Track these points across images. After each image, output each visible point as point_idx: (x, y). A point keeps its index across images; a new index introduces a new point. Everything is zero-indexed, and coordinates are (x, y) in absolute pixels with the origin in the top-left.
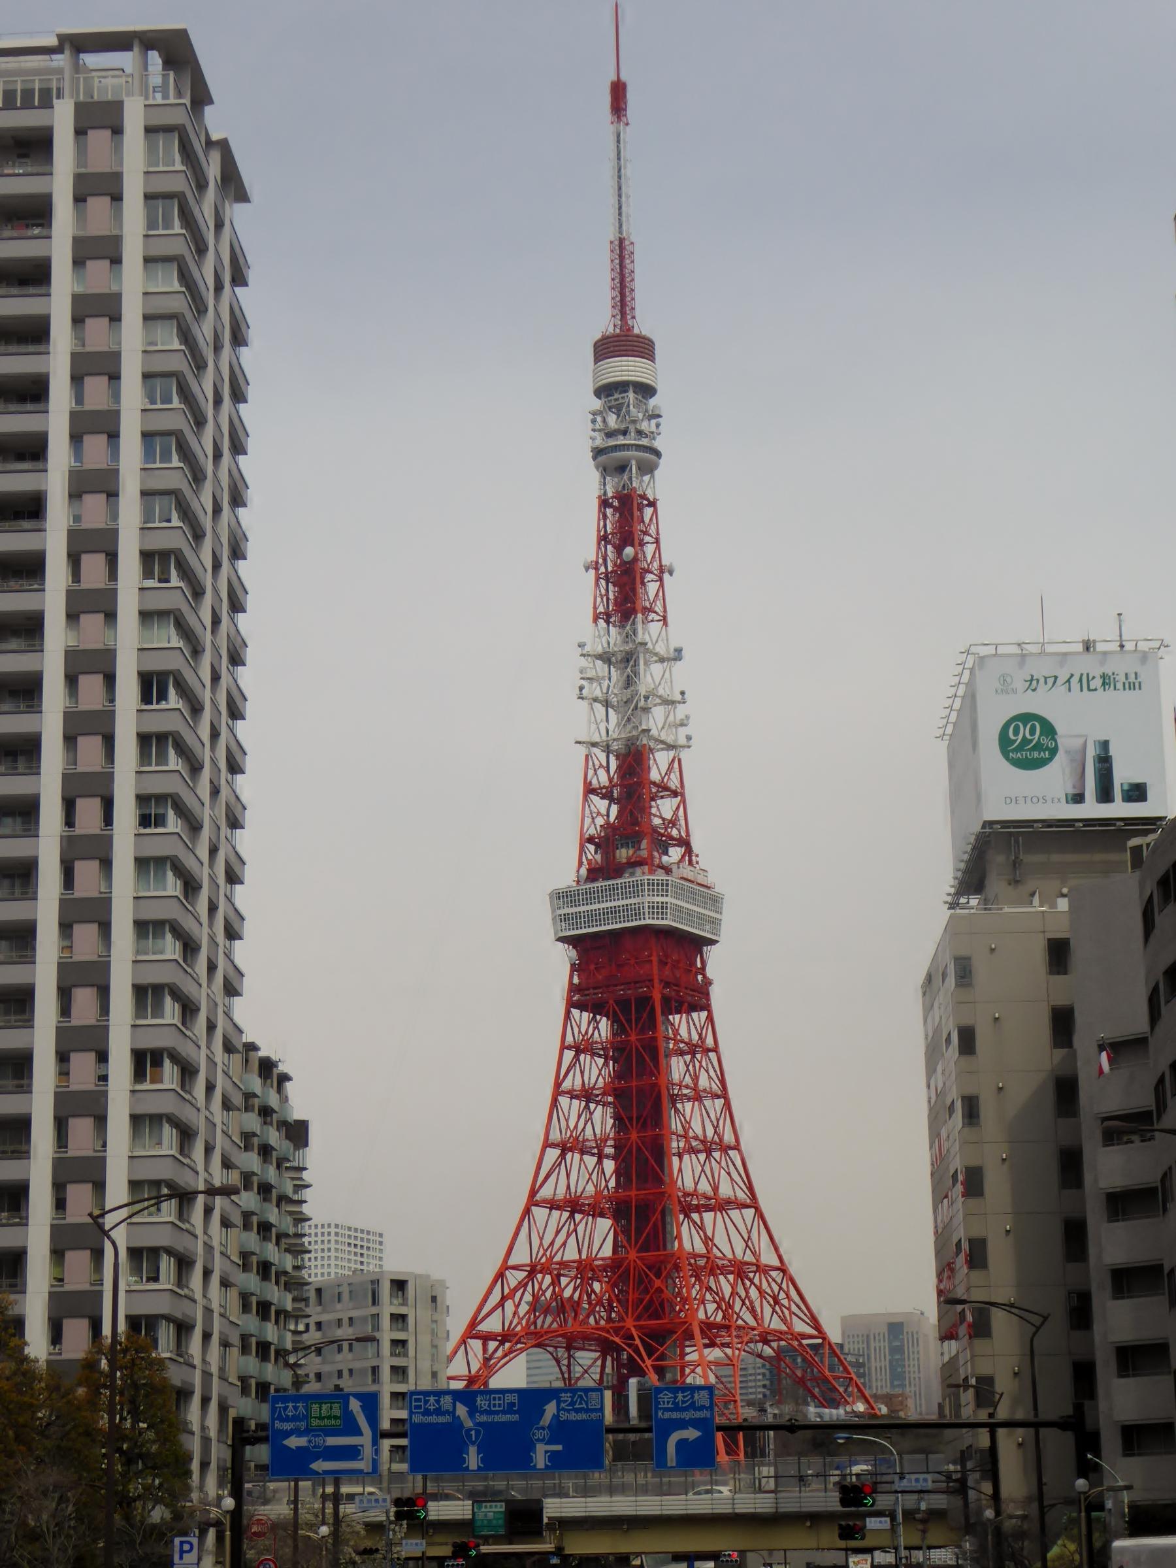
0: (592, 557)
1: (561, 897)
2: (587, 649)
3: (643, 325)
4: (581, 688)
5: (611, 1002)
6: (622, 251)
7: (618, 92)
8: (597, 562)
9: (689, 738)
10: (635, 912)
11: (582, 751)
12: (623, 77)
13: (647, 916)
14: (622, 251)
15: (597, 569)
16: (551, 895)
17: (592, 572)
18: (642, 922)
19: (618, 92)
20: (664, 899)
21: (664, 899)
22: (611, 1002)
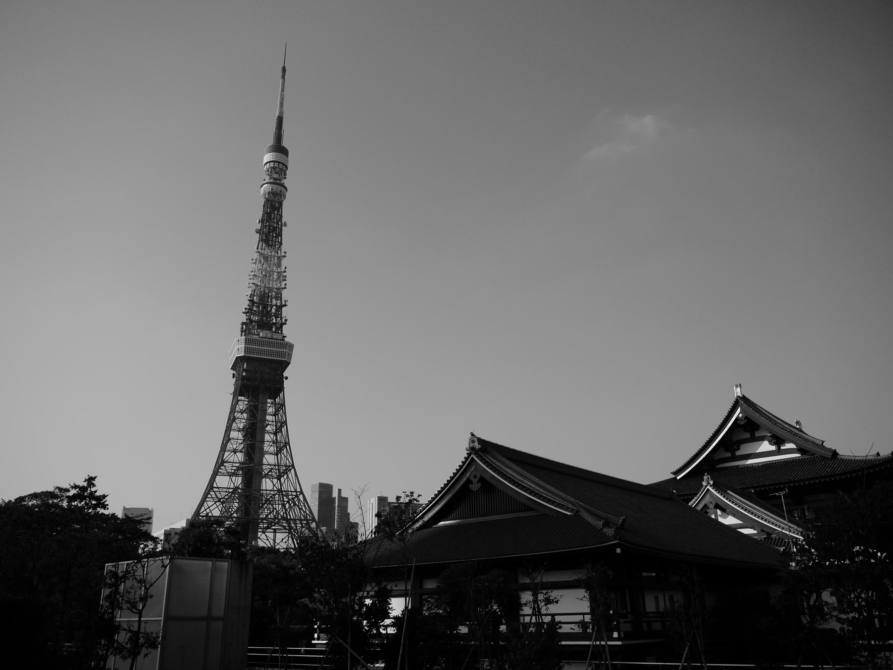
7: (284, 70)
10: (282, 354)
18: (284, 359)
19: (284, 70)
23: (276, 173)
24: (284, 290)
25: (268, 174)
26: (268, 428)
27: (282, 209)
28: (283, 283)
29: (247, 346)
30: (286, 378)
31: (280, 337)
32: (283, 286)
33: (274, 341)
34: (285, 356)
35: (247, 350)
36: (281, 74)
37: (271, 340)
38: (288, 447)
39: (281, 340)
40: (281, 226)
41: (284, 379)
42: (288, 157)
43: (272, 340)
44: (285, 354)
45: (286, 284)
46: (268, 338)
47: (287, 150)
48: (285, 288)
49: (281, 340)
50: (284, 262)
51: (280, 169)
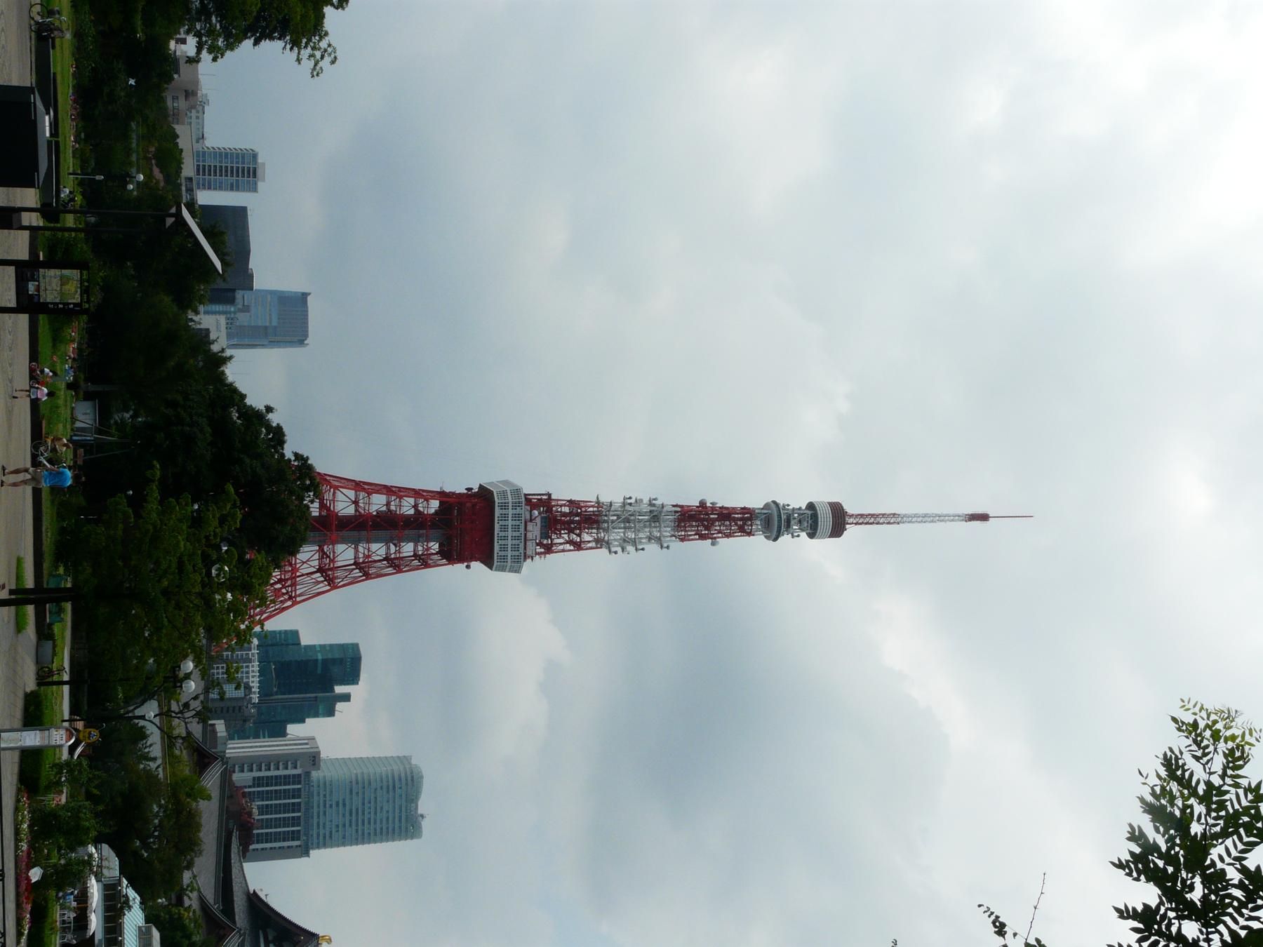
3: (851, 531)
4: (630, 498)
6: (891, 519)
7: (984, 517)
12: (990, 519)
14: (891, 519)
19: (984, 517)
24: (607, 551)
27: (744, 536)
28: (619, 549)
30: (468, 567)
31: (529, 552)
32: (613, 549)
38: (364, 578)
39: (525, 553)
40: (712, 538)
41: (466, 564)
45: (616, 553)
46: (525, 535)
48: (610, 552)
49: (525, 553)
50: (652, 548)
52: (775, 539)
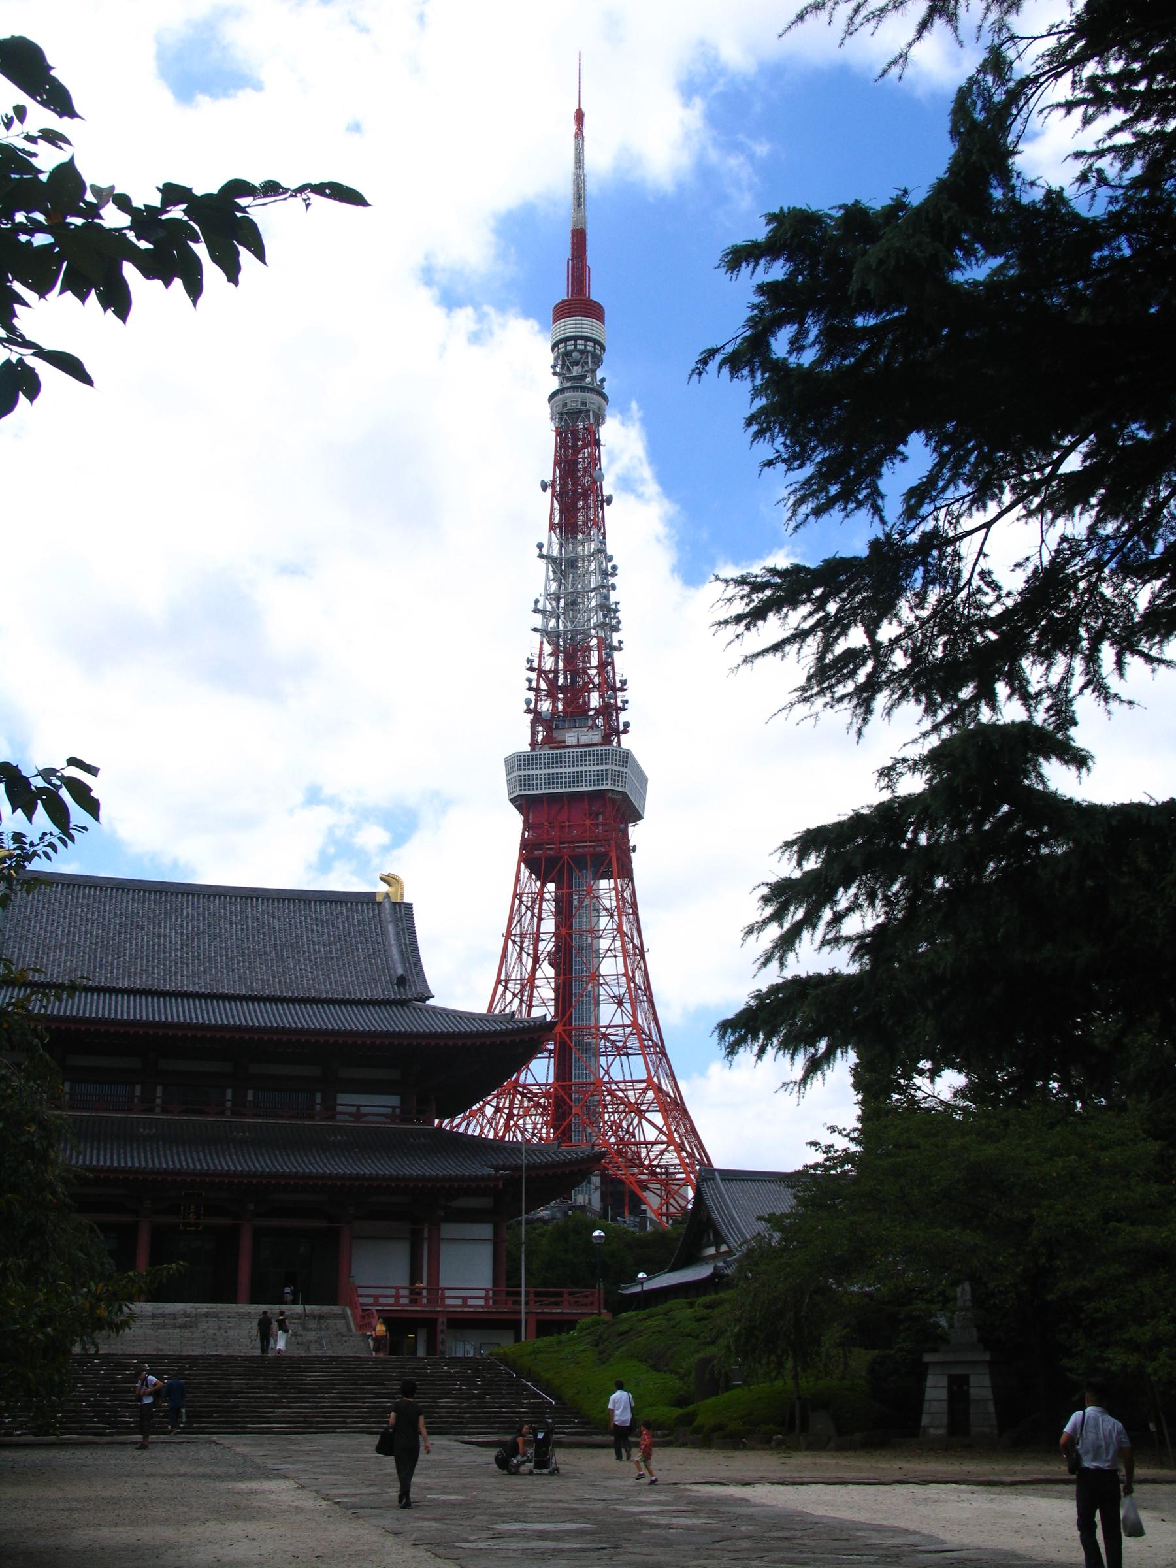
0: (548, 478)
1: (516, 762)
2: (545, 552)
5: (566, 857)
7: (579, 117)
8: (554, 481)
9: (620, 642)
10: (600, 777)
11: (538, 636)
13: (609, 782)
15: (553, 488)
16: (508, 762)
17: (549, 491)
19: (579, 117)
20: (625, 770)
21: (625, 770)
22: (566, 857)
23: (576, 363)
25: (555, 374)
26: (604, 944)
29: (523, 773)
33: (583, 750)
34: (607, 779)
35: (525, 782)
36: (573, 128)
37: (575, 750)
42: (603, 323)
43: (579, 750)
44: (606, 775)
47: (599, 305)
51: (581, 352)
52: (604, 397)
